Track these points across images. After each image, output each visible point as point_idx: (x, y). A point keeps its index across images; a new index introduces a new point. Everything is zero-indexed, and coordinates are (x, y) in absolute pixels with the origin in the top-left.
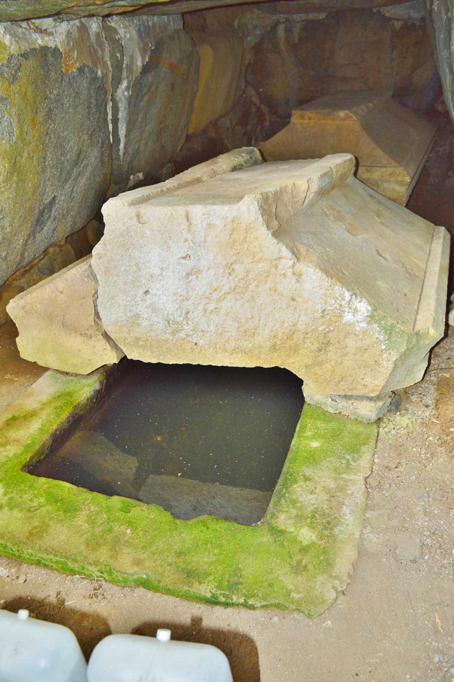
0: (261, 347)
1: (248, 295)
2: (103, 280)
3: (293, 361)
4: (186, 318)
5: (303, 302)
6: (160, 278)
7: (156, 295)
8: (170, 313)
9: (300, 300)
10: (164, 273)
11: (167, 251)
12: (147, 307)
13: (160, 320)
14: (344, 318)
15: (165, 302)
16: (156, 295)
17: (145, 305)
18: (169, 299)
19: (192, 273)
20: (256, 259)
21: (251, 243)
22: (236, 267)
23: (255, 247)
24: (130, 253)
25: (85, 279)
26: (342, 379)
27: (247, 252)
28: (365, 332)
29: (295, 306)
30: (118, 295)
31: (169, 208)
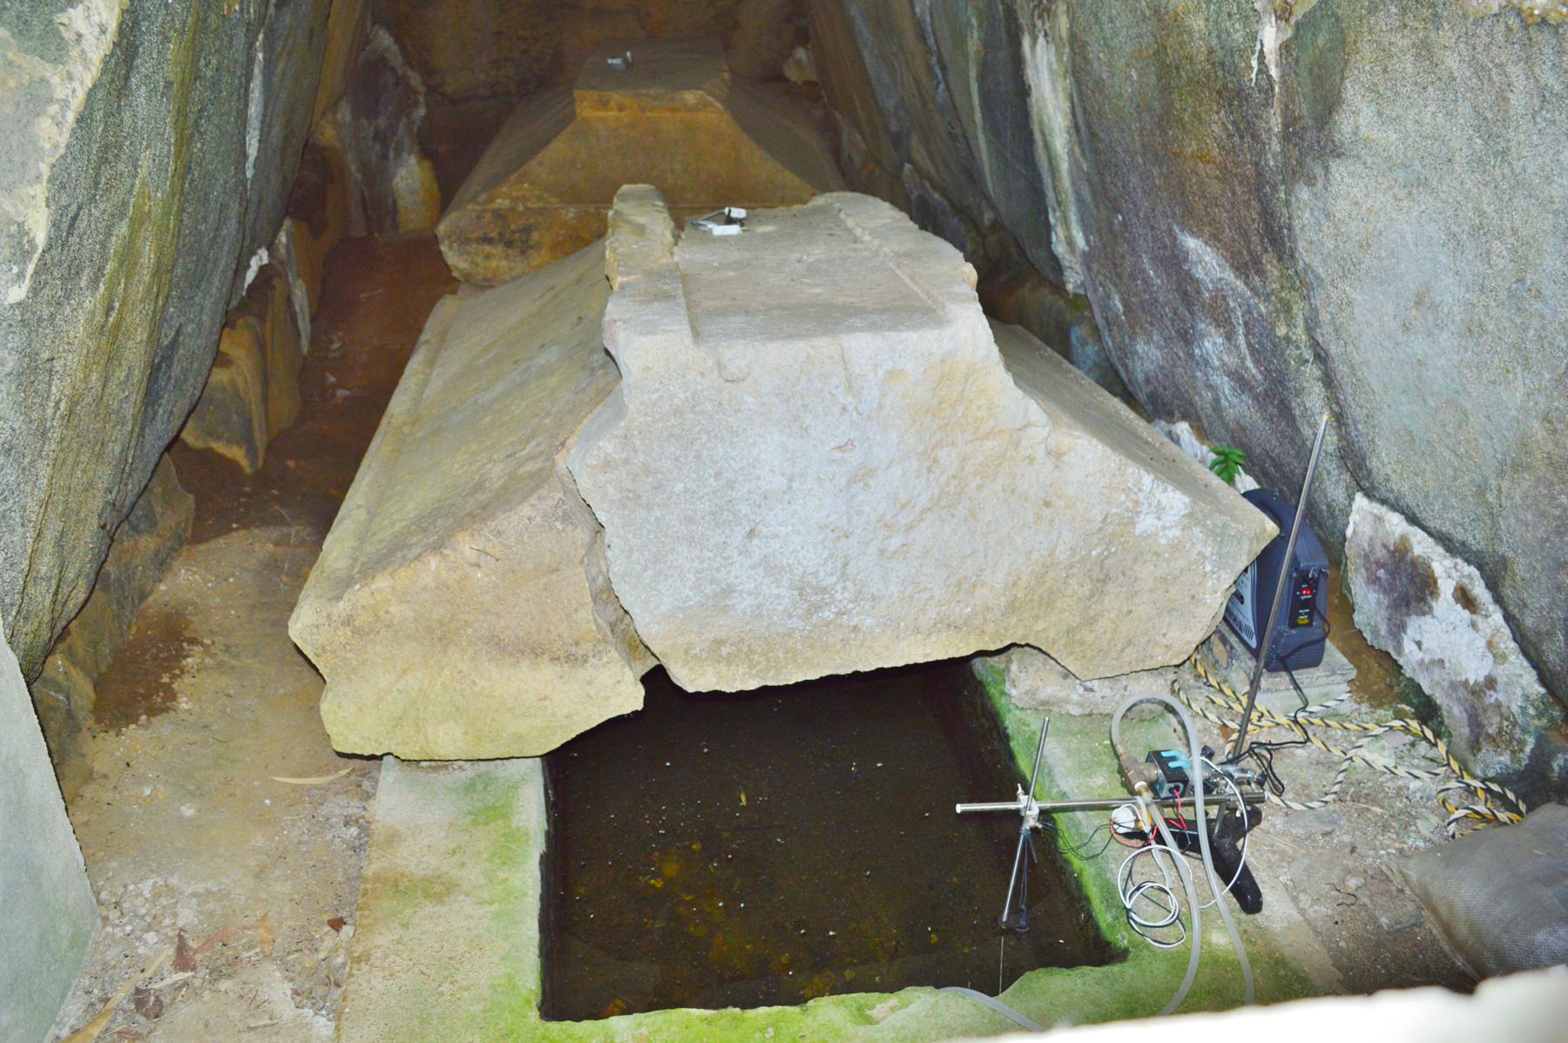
0: (988, 609)
2: (616, 520)
4: (844, 577)
6: (787, 497)
8: (809, 570)
9: (1060, 503)
10: (795, 485)
12: (753, 567)
13: (783, 591)
19: (862, 476)
22: (942, 454)
23: (979, 408)
26: (1129, 643)
28: (1175, 546)
30: (673, 550)
31: (801, 344)
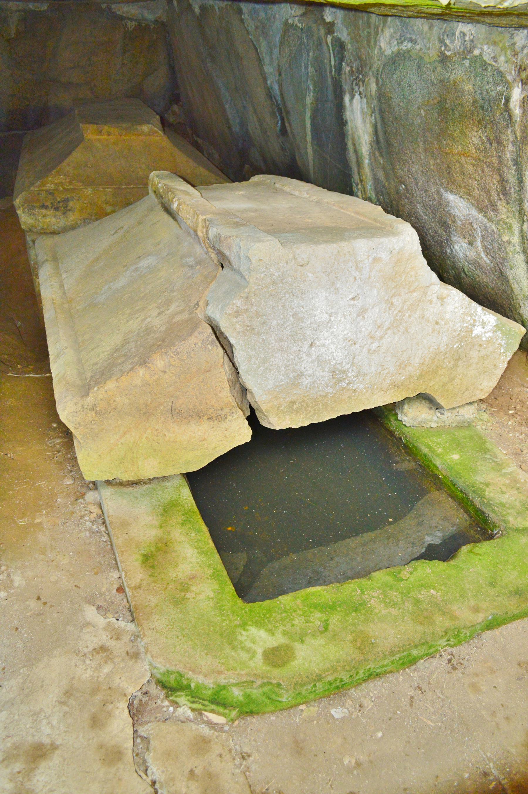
0: (411, 377)
1: (403, 327)
2: (241, 342)
3: (433, 384)
4: (353, 365)
5: (445, 324)
6: (329, 325)
7: (323, 345)
8: (338, 362)
10: (332, 318)
11: (336, 293)
12: (312, 362)
13: (325, 374)
14: (474, 332)
15: (334, 351)
16: (323, 345)
17: (310, 360)
18: (339, 347)
19: (362, 312)
20: (412, 288)
21: (408, 273)
22: (394, 300)
23: (411, 277)
24: (284, 303)
25: (209, 346)
26: (467, 389)
27: (404, 283)
28: (489, 341)
29: (438, 329)
30: (273, 356)
31: (335, 245)
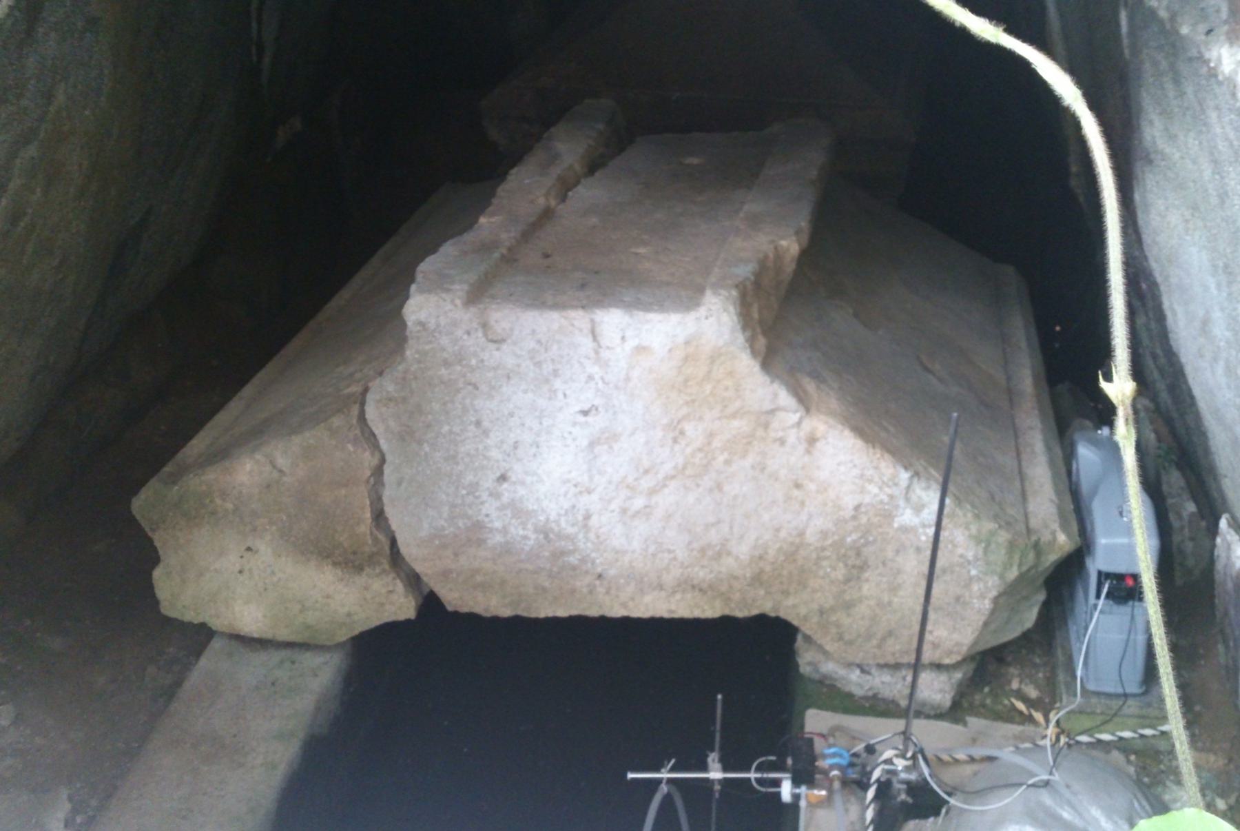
9: (812, 487)
19: (605, 439)
21: (719, 381)
22: (689, 428)
